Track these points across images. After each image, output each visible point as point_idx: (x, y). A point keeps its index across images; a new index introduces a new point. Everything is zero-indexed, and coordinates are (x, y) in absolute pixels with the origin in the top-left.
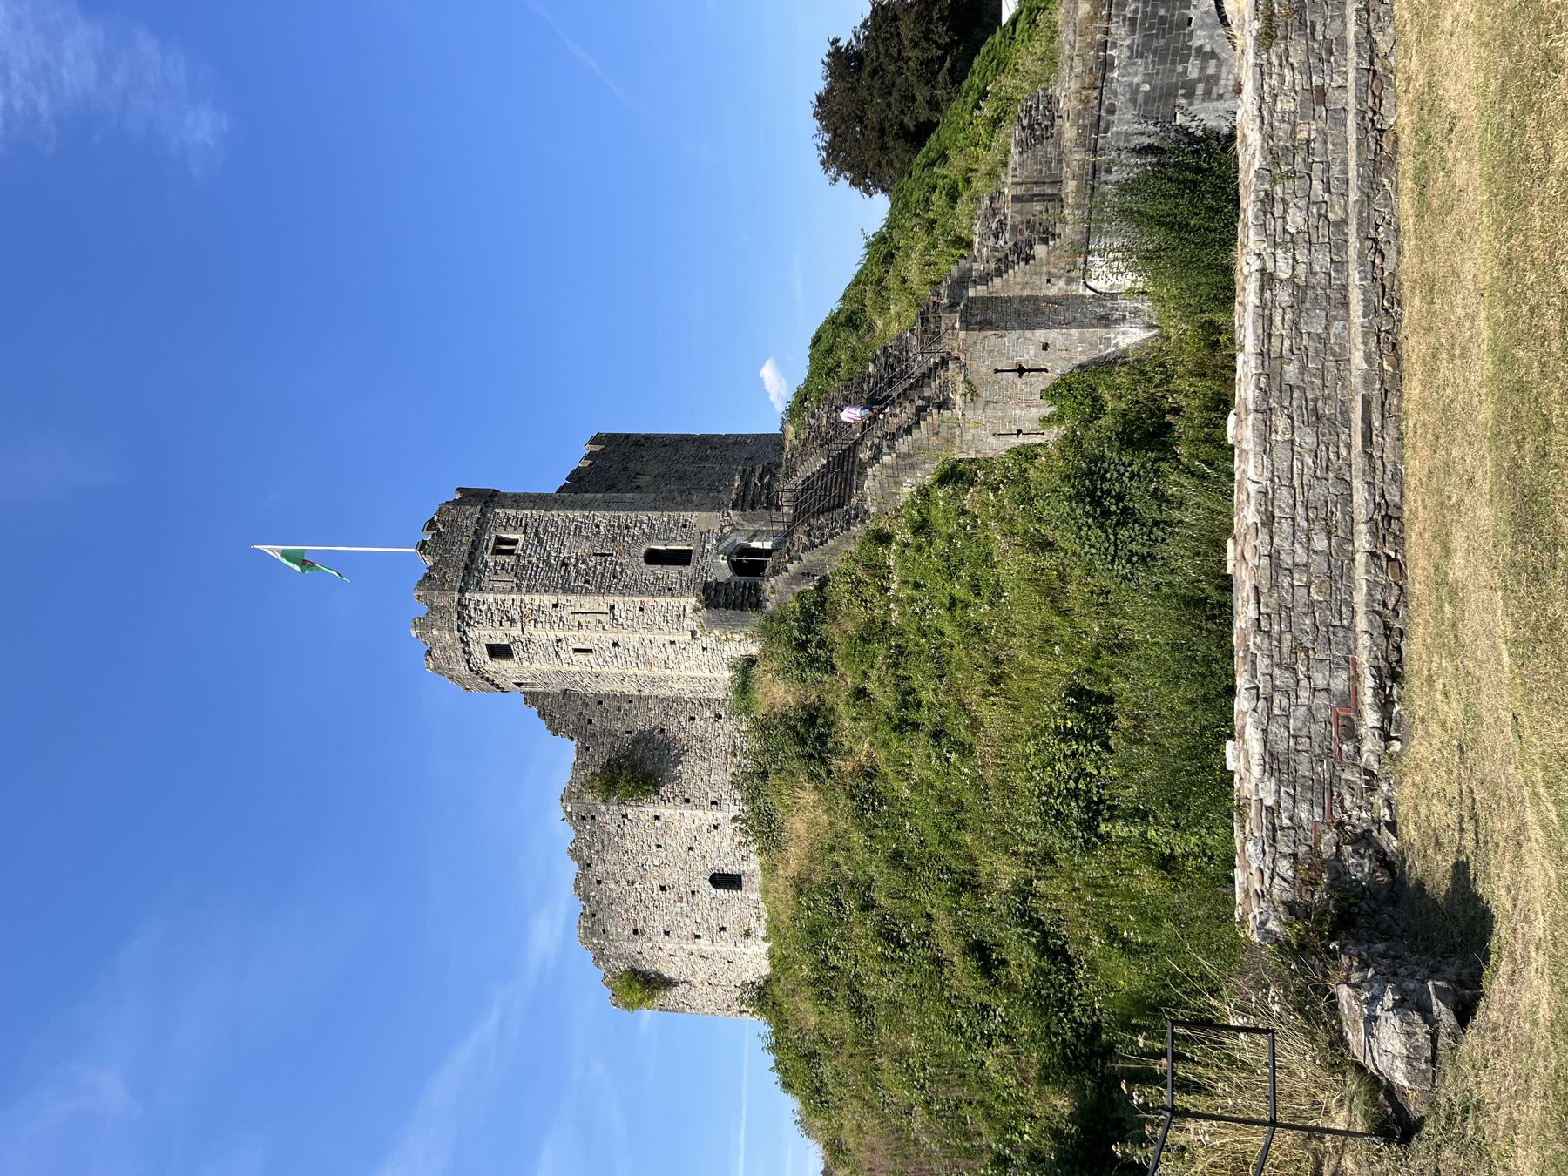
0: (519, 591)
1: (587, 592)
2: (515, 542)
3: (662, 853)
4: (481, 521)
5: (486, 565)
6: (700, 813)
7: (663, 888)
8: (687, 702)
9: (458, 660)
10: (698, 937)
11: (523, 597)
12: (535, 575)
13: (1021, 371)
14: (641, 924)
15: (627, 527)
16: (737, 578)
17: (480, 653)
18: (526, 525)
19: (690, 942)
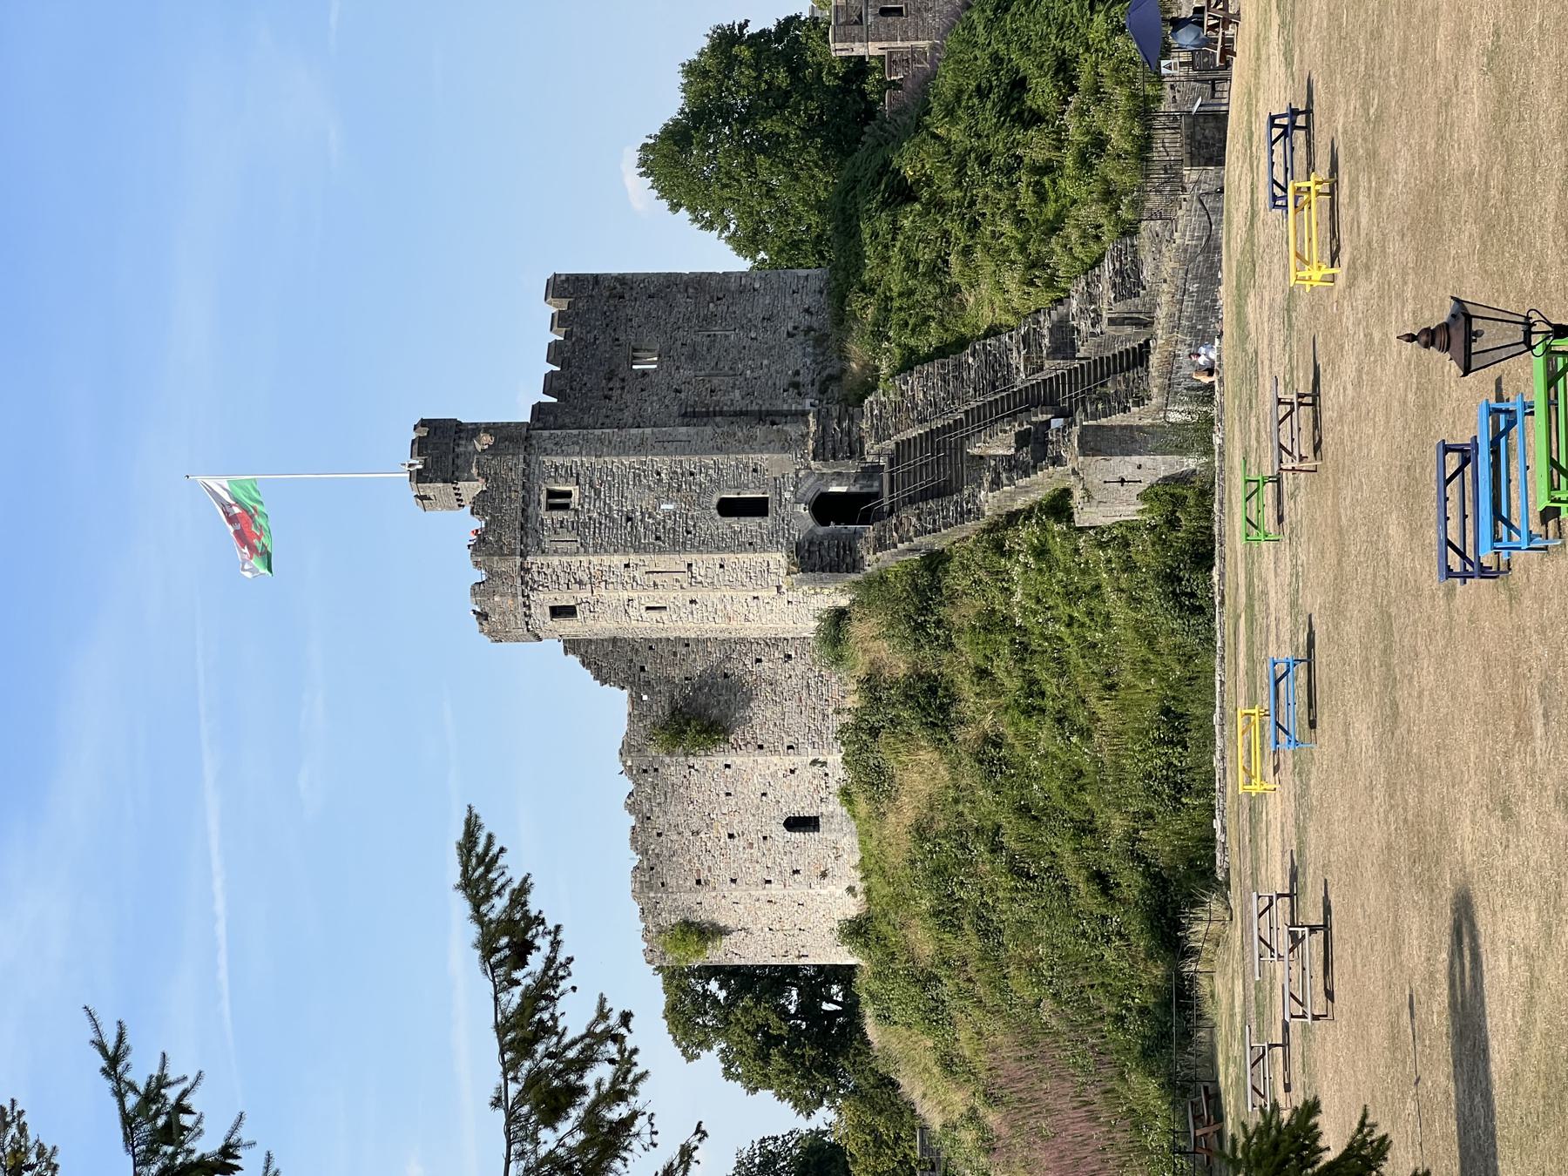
0: (586, 551)
1: (661, 551)
2: (568, 495)
3: (732, 801)
4: (527, 472)
5: (542, 524)
6: (775, 759)
7: (731, 836)
8: (752, 643)
9: (516, 623)
10: (769, 882)
11: (591, 558)
12: (600, 533)
13: (1122, 481)
14: (704, 875)
15: (692, 474)
16: (821, 530)
17: (540, 614)
18: (578, 475)
19: (760, 888)
